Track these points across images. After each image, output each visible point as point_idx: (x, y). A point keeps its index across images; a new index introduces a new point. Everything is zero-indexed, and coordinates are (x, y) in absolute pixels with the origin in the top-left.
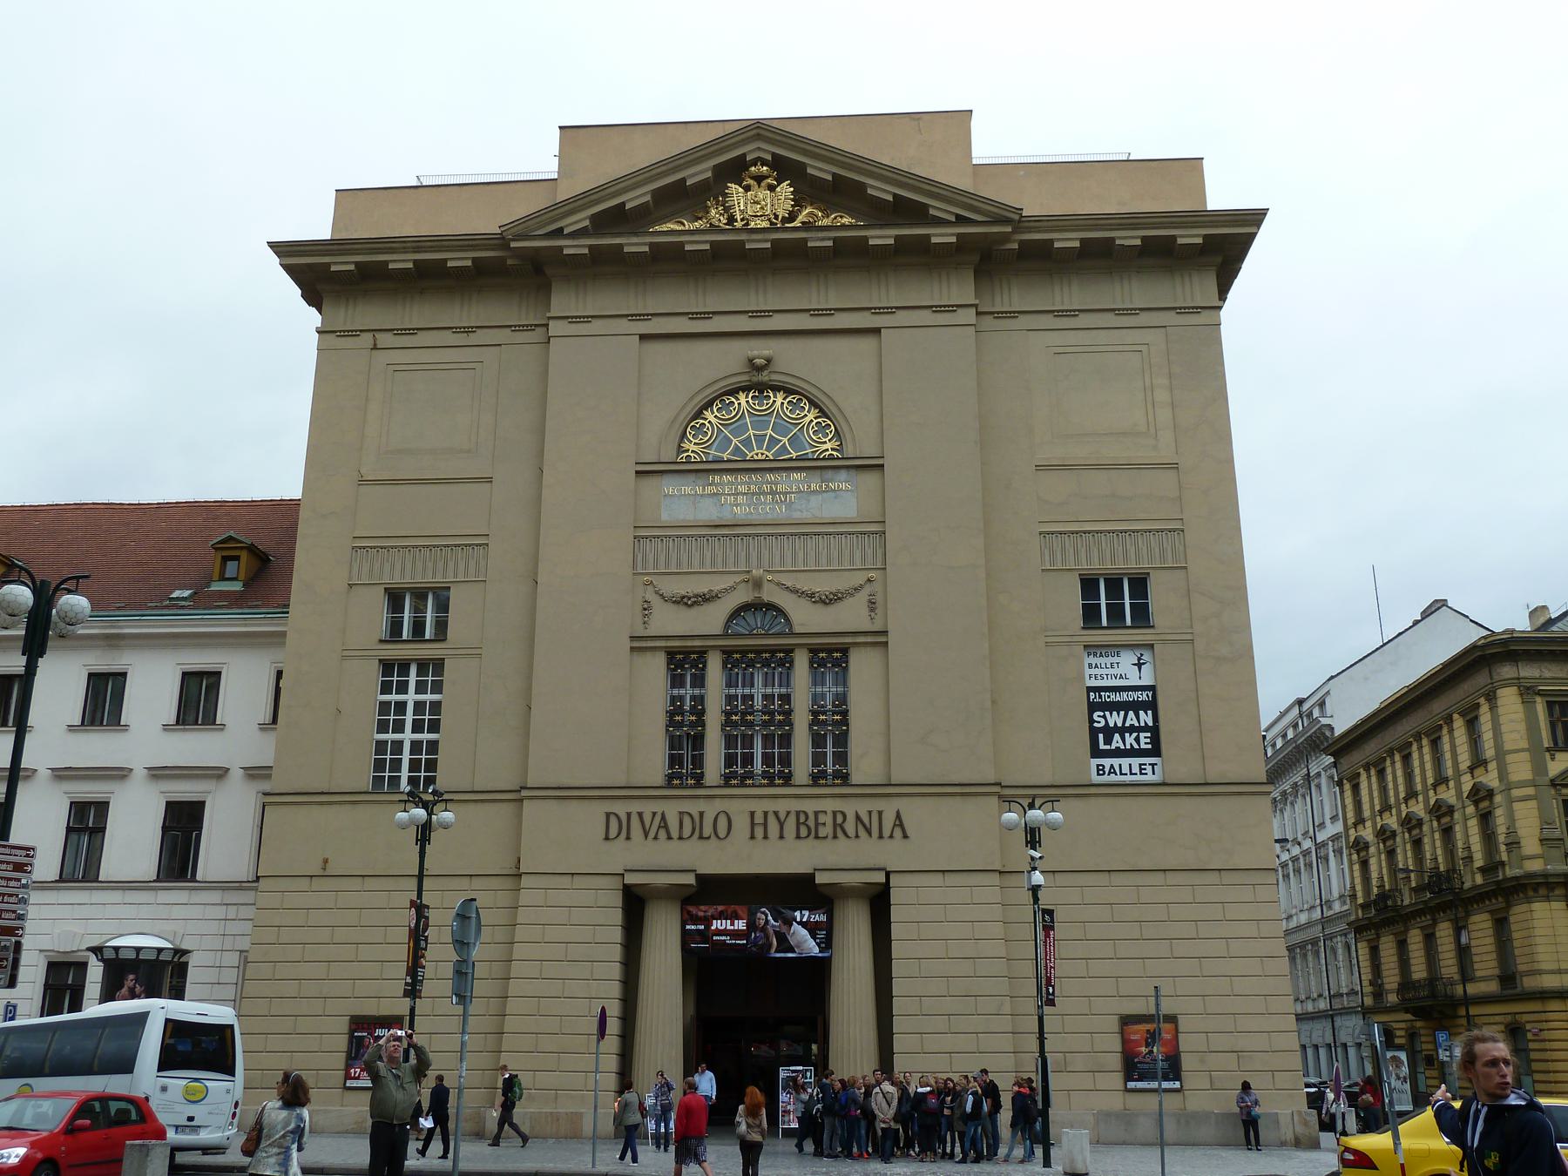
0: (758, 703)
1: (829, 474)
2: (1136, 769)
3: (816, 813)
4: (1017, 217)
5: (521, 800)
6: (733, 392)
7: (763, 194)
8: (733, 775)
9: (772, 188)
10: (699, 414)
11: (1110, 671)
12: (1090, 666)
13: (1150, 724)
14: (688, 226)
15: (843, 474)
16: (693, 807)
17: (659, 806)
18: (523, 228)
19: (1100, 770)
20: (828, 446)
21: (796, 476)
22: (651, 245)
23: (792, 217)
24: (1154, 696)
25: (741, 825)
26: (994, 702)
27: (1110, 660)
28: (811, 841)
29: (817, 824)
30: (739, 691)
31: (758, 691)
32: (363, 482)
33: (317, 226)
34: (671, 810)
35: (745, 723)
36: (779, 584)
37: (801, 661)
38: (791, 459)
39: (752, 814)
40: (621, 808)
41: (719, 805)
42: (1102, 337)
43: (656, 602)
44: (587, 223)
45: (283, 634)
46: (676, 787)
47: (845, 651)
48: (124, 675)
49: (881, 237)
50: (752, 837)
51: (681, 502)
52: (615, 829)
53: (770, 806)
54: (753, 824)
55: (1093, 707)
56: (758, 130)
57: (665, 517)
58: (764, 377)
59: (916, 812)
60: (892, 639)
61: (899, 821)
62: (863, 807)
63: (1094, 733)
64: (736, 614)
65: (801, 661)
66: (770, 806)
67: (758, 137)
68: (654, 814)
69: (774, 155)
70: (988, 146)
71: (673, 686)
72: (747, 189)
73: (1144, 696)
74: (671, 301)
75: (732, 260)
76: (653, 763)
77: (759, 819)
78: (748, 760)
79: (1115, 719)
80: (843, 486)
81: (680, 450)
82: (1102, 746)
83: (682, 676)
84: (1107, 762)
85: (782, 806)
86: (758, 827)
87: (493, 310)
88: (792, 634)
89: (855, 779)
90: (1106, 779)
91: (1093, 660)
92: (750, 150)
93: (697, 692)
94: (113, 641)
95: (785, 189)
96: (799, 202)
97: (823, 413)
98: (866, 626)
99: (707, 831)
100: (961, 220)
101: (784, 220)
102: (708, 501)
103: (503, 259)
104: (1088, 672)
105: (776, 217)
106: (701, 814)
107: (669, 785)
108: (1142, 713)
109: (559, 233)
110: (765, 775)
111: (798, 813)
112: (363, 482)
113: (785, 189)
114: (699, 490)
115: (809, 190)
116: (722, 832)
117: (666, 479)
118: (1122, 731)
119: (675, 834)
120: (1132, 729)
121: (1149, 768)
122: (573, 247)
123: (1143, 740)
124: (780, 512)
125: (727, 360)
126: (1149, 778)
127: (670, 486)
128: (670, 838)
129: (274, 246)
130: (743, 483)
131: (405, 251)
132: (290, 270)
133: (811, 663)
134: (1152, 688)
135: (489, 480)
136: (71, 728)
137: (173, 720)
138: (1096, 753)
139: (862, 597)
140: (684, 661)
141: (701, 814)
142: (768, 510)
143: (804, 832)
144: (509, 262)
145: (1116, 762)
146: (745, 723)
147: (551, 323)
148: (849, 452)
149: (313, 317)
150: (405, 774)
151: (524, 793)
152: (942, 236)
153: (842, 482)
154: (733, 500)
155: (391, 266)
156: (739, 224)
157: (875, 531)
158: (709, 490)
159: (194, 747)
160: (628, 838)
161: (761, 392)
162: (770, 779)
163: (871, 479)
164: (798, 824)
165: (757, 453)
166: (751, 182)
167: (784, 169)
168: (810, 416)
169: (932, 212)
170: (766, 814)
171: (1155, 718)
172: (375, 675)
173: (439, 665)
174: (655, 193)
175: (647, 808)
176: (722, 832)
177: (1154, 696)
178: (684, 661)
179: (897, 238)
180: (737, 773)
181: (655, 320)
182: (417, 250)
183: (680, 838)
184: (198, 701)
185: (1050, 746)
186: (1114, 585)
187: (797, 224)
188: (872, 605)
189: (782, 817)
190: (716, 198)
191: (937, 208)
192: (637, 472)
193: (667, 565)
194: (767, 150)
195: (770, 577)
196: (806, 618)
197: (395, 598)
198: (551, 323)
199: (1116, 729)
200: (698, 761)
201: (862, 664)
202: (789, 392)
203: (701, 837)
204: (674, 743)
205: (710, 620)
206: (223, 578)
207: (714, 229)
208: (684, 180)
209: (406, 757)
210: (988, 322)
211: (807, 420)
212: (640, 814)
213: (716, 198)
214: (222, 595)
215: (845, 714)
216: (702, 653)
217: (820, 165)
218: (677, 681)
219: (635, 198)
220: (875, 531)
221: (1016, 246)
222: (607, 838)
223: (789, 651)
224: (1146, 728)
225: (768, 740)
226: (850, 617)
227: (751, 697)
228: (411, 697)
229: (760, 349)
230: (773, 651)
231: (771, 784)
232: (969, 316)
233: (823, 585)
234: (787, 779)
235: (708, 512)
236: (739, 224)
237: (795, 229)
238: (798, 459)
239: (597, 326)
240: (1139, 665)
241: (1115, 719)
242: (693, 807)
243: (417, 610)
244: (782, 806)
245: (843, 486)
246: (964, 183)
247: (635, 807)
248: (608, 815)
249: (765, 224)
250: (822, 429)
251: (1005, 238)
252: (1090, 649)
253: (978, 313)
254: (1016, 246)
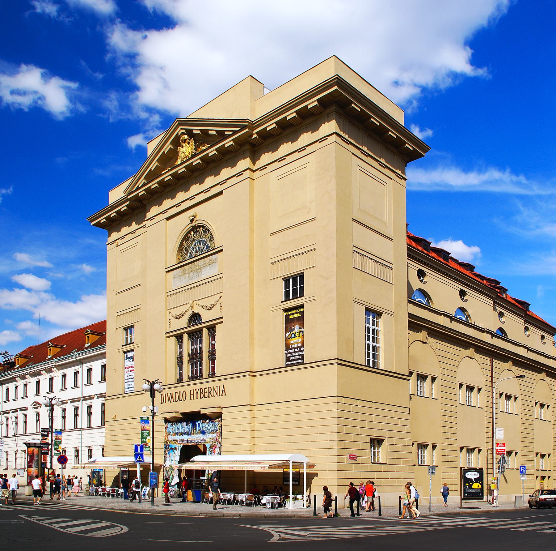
37: (205, 331)
59: (229, 385)
61: (224, 390)
65: (205, 331)
88: (202, 323)
136: (100, 382)
139: (219, 304)
186: (294, 278)
192: (167, 272)
196: (206, 316)
205: (183, 322)
227: (196, 349)
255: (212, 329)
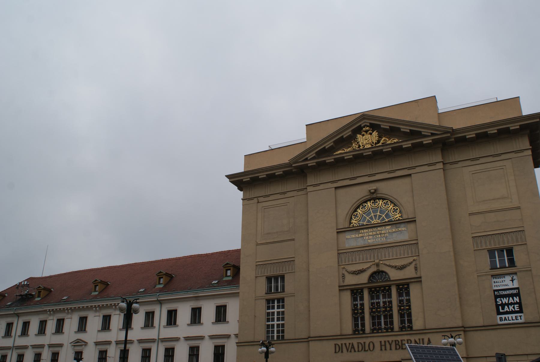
0: (382, 304)
1: (398, 225)
2: (514, 318)
3: (402, 341)
4: (451, 131)
5: (308, 341)
6: (366, 202)
7: (368, 136)
8: (375, 329)
9: (371, 134)
10: (355, 211)
11: (502, 284)
12: (494, 282)
13: (518, 301)
14: (346, 150)
15: (402, 225)
16: (362, 341)
17: (351, 341)
18: (295, 160)
19: (501, 319)
20: (398, 216)
21: (388, 227)
22: (334, 159)
23: (378, 142)
24: (519, 291)
25: (377, 346)
26: (460, 298)
27: (501, 280)
28: (401, 351)
29: (402, 344)
30: (375, 301)
31: (381, 300)
32: (258, 244)
33: (240, 168)
34: (355, 342)
35: (377, 311)
36: (385, 264)
38: (386, 222)
39: (381, 342)
40: (339, 342)
41: (370, 340)
42: (489, 165)
43: (346, 274)
44: (314, 155)
45: (238, 293)
46: (357, 334)
47: (408, 284)
48: (201, 308)
49: (407, 144)
50: (381, 350)
51: (352, 240)
52: (338, 349)
53: (387, 339)
54: (381, 345)
55: (496, 297)
56: (364, 116)
57: (347, 246)
58: (374, 196)
60: (423, 279)
62: (417, 338)
63: (497, 306)
64: (372, 275)
66: (387, 339)
67: (364, 119)
68: (350, 344)
69: (370, 123)
70: (443, 106)
71: (354, 301)
72: (363, 135)
73: (515, 292)
74: (344, 175)
75: (360, 159)
76: (348, 328)
77: (383, 343)
78: (380, 324)
79: (505, 301)
80: (403, 229)
81: (350, 223)
82: (501, 311)
83: (357, 298)
84: (503, 316)
85: (390, 339)
86: (383, 347)
87: (292, 185)
89: (414, 328)
90: (503, 322)
91: (495, 280)
92: (362, 123)
93: (361, 302)
94: (197, 298)
95: (375, 134)
96: (380, 137)
97: (395, 205)
98: (414, 275)
99: (367, 348)
100: (433, 134)
101: (376, 144)
102: (360, 239)
103: (292, 170)
104: (494, 284)
105: (373, 143)
106: (364, 343)
107: (354, 334)
108: (515, 298)
109: (306, 160)
110: (385, 328)
111: (395, 341)
112: (258, 244)
113: (375, 134)
114: (357, 236)
115: (383, 132)
116: (371, 349)
117: (347, 233)
118: (508, 305)
119: (357, 350)
120: (511, 304)
121: (519, 318)
122: (311, 163)
123: (516, 308)
124: (384, 240)
125: (362, 192)
126: (520, 321)
127: (348, 236)
128: (355, 351)
129: (227, 176)
130: (370, 232)
131: (263, 172)
132: (232, 182)
133: (397, 290)
134: (518, 288)
135: (293, 240)
137: (214, 321)
138: (499, 313)
139: (412, 266)
140: (356, 292)
141: (364, 343)
142: (380, 240)
143: (398, 347)
144: (293, 170)
145: (506, 316)
146: (377, 311)
147: (308, 188)
148: (405, 217)
149: (241, 194)
150: (275, 334)
151: (310, 339)
152: (427, 141)
153: (402, 228)
154: (369, 238)
155: (260, 177)
156: (361, 148)
157: (414, 244)
158: (360, 235)
159: (221, 329)
160: (342, 352)
161: (375, 200)
162: (387, 330)
163: (412, 226)
164: (396, 344)
165: (375, 221)
166: (364, 133)
167: (374, 127)
168: (391, 207)
169: (423, 133)
170: (385, 342)
171: (520, 299)
172: (263, 303)
173: (283, 300)
174: (334, 142)
175: (347, 342)
176: (371, 349)
177: (519, 291)
178: (356, 292)
179: (412, 144)
180: (376, 329)
181: (339, 182)
182: (267, 171)
183: (358, 351)
184: (221, 314)
185: (480, 312)
187: (380, 144)
188: (416, 268)
189: (390, 342)
190: (354, 140)
191: (424, 132)
193: (349, 261)
194: (367, 122)
195: (381, 262)
196: (394, 275)
197: (269, 279)
198: (308, 188)
199: (506, 304)
200: (363, 325)
201: (414, 290)
202: (383, 199)
203: (365, 351)
204: (355, 319)
205: (364, 278)
206: (226, 276)
207: (354, 150)
208: (343, 136)
209: (275, 329)
210: (448, 166)
211: (390, 208)
212: (345, 344)
213: (354, 140)
214: (226, 281)
215: (410, 306)
216: (362, 290)
217: (385, 124)
218: (355, 299)
219: (328, 145)
220: (414, 244)
221: (453, 140)
222: (335, 352)
223: (390, 286)
224: (517, 303)
225: (385, 317)
226: (409, 273)
227: (379, 303)
228: (276, 310)
229: (373, 187)
230: (385, 287)
231: (387, 332)
232: (441, 166)
233: (399, 263)
234: (392, 329)
235: (360, 243)
236: (361, 148)
237: (379, 146)
238: (388, 221)
239: (322, 187)
240: (512, 280)
241: (505, 301)
242: (362, 341)
243: (275, 282)
244: (390, 339)
245: (403, 229)
246: (434, 122)
247: (344, 342)
248: (335, 345)
249: (370, 146)
250: (395, 210)
251: (448, 138)
252: (494, 276)
253: (444, 164)
254: (453, 140)
255: (404, 288)
